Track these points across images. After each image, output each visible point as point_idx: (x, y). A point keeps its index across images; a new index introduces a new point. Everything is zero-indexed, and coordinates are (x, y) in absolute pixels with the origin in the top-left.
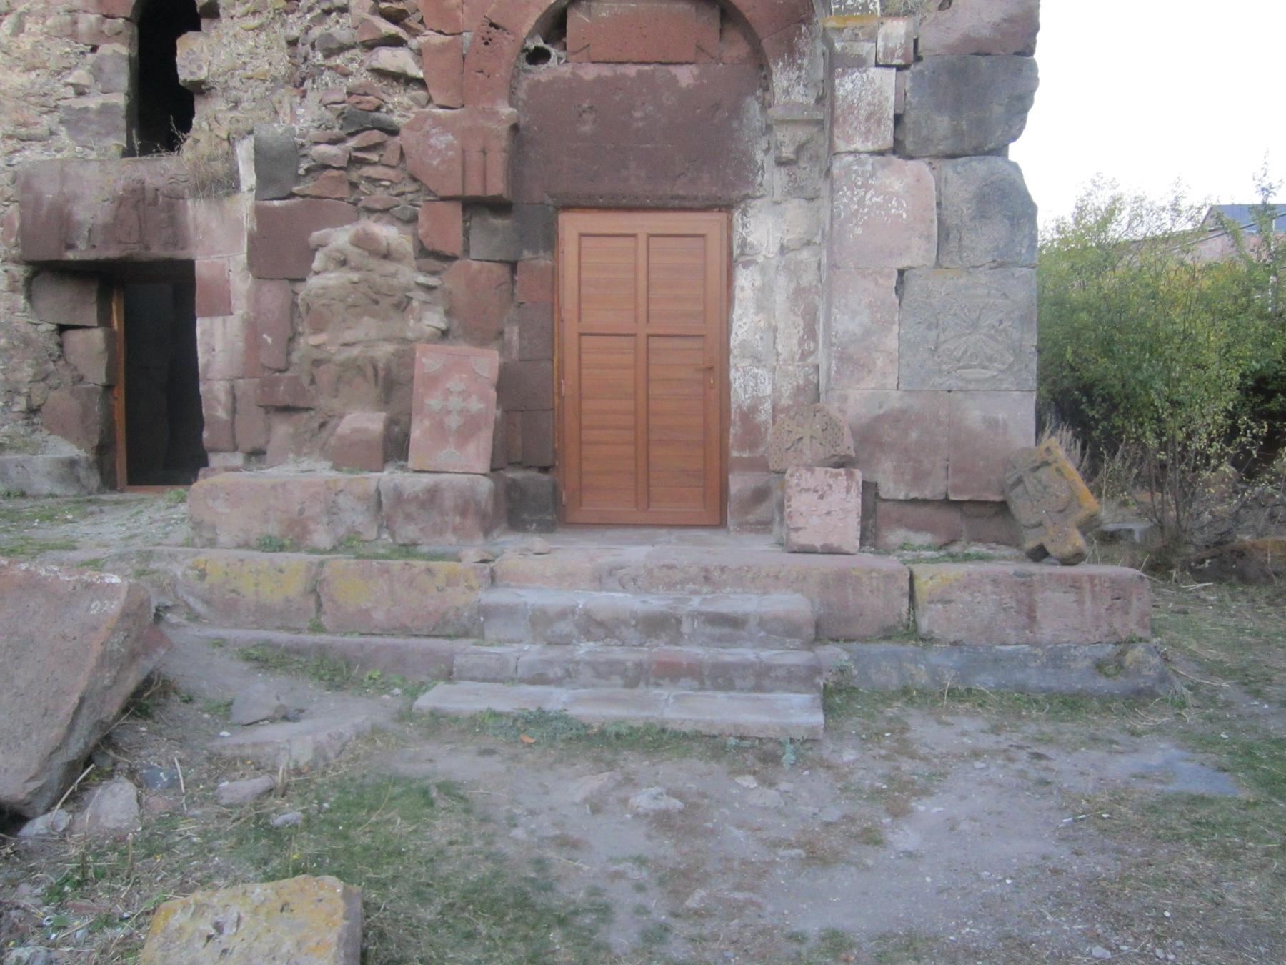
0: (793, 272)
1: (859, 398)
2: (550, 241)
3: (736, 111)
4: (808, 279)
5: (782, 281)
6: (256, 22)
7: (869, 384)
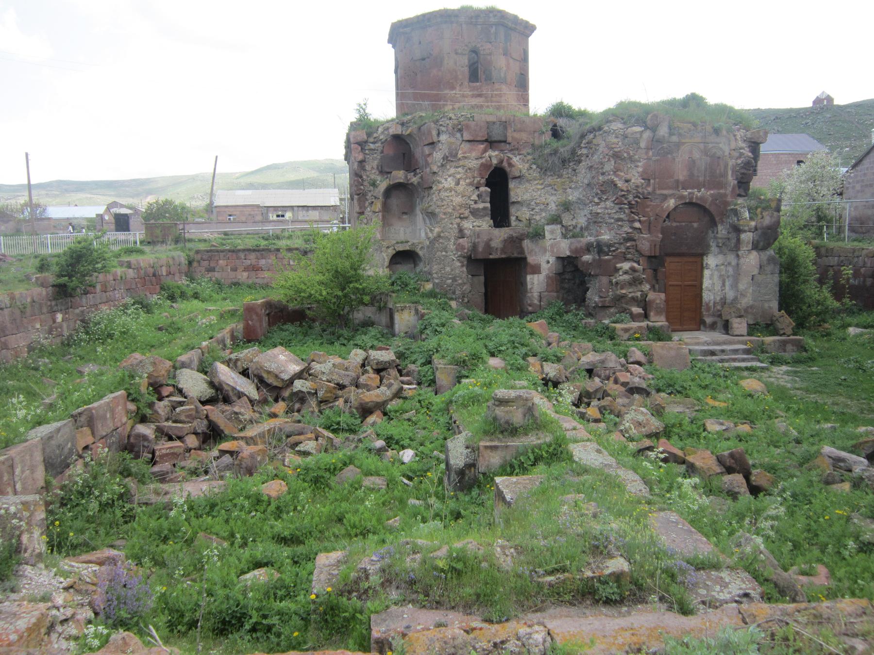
1: (745, 302)
3: (707, 233)
5: (716, 273)
6: (539, 187)
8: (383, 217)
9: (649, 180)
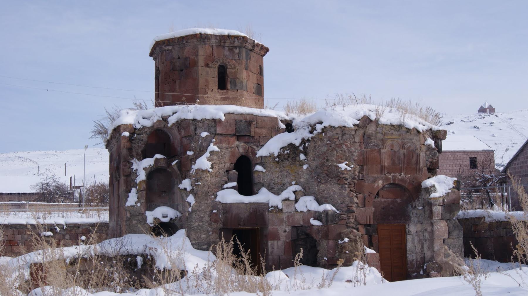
0: (419, 236)
4: (421, 238)
5: (416, 237)
7: (440, 258)
8: (147, 194)
9: (362, 166)
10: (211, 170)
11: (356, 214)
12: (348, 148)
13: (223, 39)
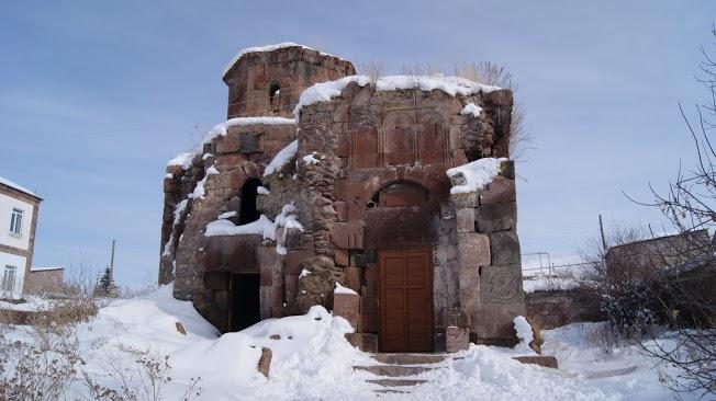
0: (452, 267)
2: (375, 260)
3: (432, 219)
7: (472, 302)
10: (203, 198)
11: (331, 232)
12: (324, 133)
13: (274, 54)
